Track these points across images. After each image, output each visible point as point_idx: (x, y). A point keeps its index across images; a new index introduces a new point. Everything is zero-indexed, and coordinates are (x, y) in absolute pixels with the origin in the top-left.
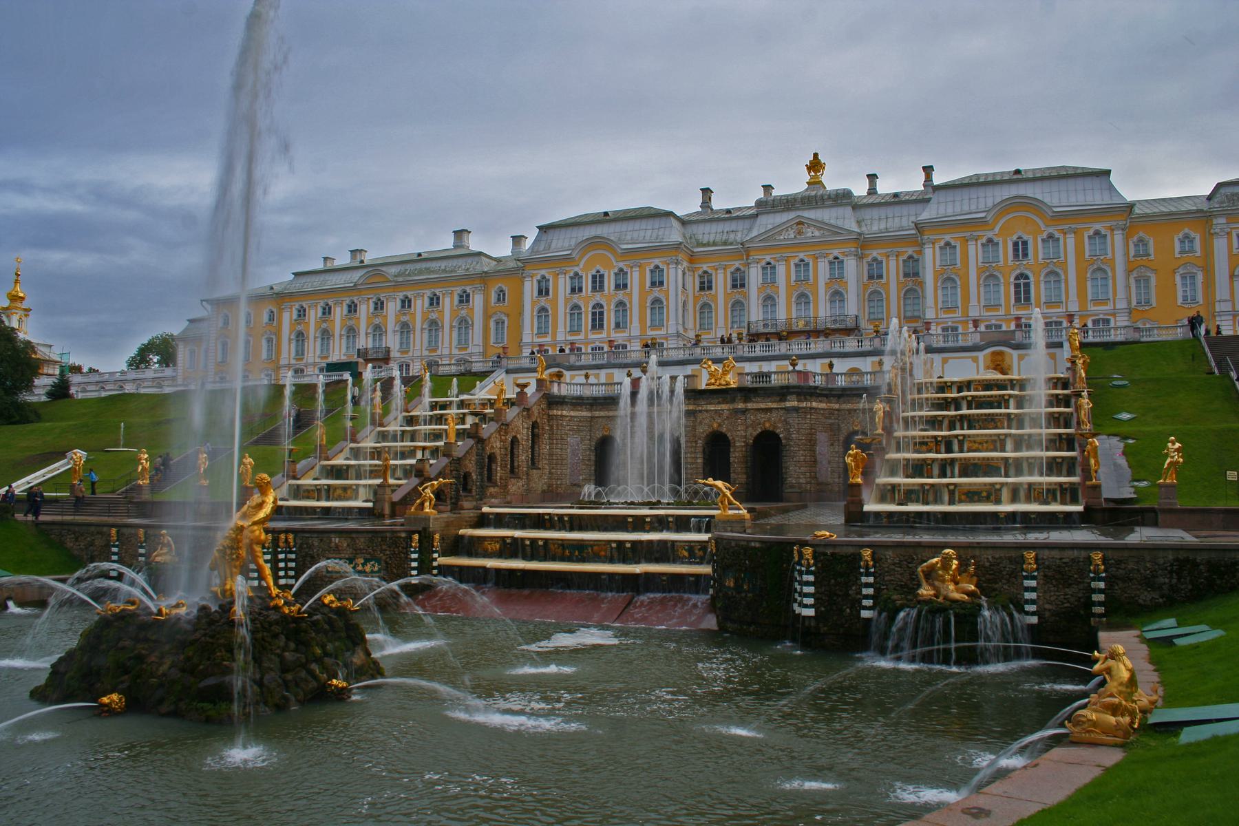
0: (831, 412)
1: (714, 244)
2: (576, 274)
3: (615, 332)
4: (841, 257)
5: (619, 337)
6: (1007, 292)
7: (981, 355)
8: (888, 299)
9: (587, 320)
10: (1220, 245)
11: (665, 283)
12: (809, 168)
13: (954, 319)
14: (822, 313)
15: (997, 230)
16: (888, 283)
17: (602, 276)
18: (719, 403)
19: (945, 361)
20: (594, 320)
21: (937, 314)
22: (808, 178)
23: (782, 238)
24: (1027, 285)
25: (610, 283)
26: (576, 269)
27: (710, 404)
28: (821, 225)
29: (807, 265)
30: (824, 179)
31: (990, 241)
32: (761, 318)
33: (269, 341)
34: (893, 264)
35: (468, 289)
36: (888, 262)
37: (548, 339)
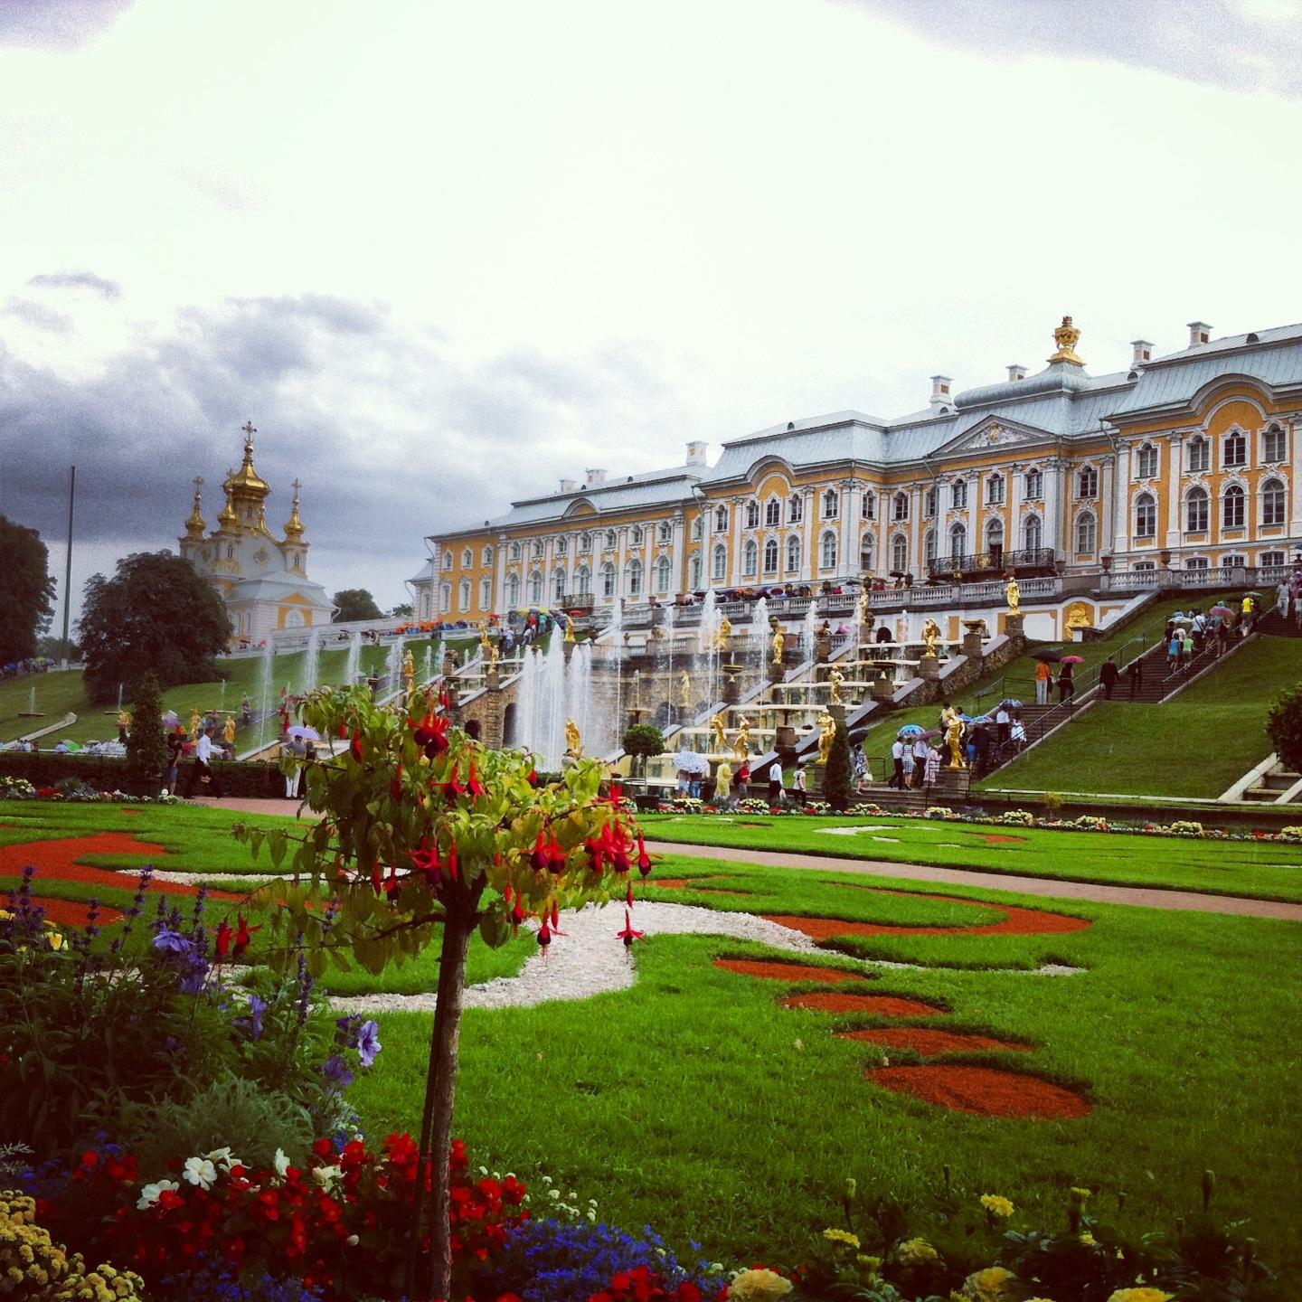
4: (1038, 469)
7: (1059, 608)
13: (1151, 553)
15: (1206, 424)
17: (777, 506)
20: (768, 560)
21: (1129, 548)
23: (974, 446)
24: (1240, 501)
25: (786, 513)
26: (752, 497)
28: (1016, 427)
29: (1003, 480)
30: (1080, 351)
33: (487, 585)
36: (1102, 470)
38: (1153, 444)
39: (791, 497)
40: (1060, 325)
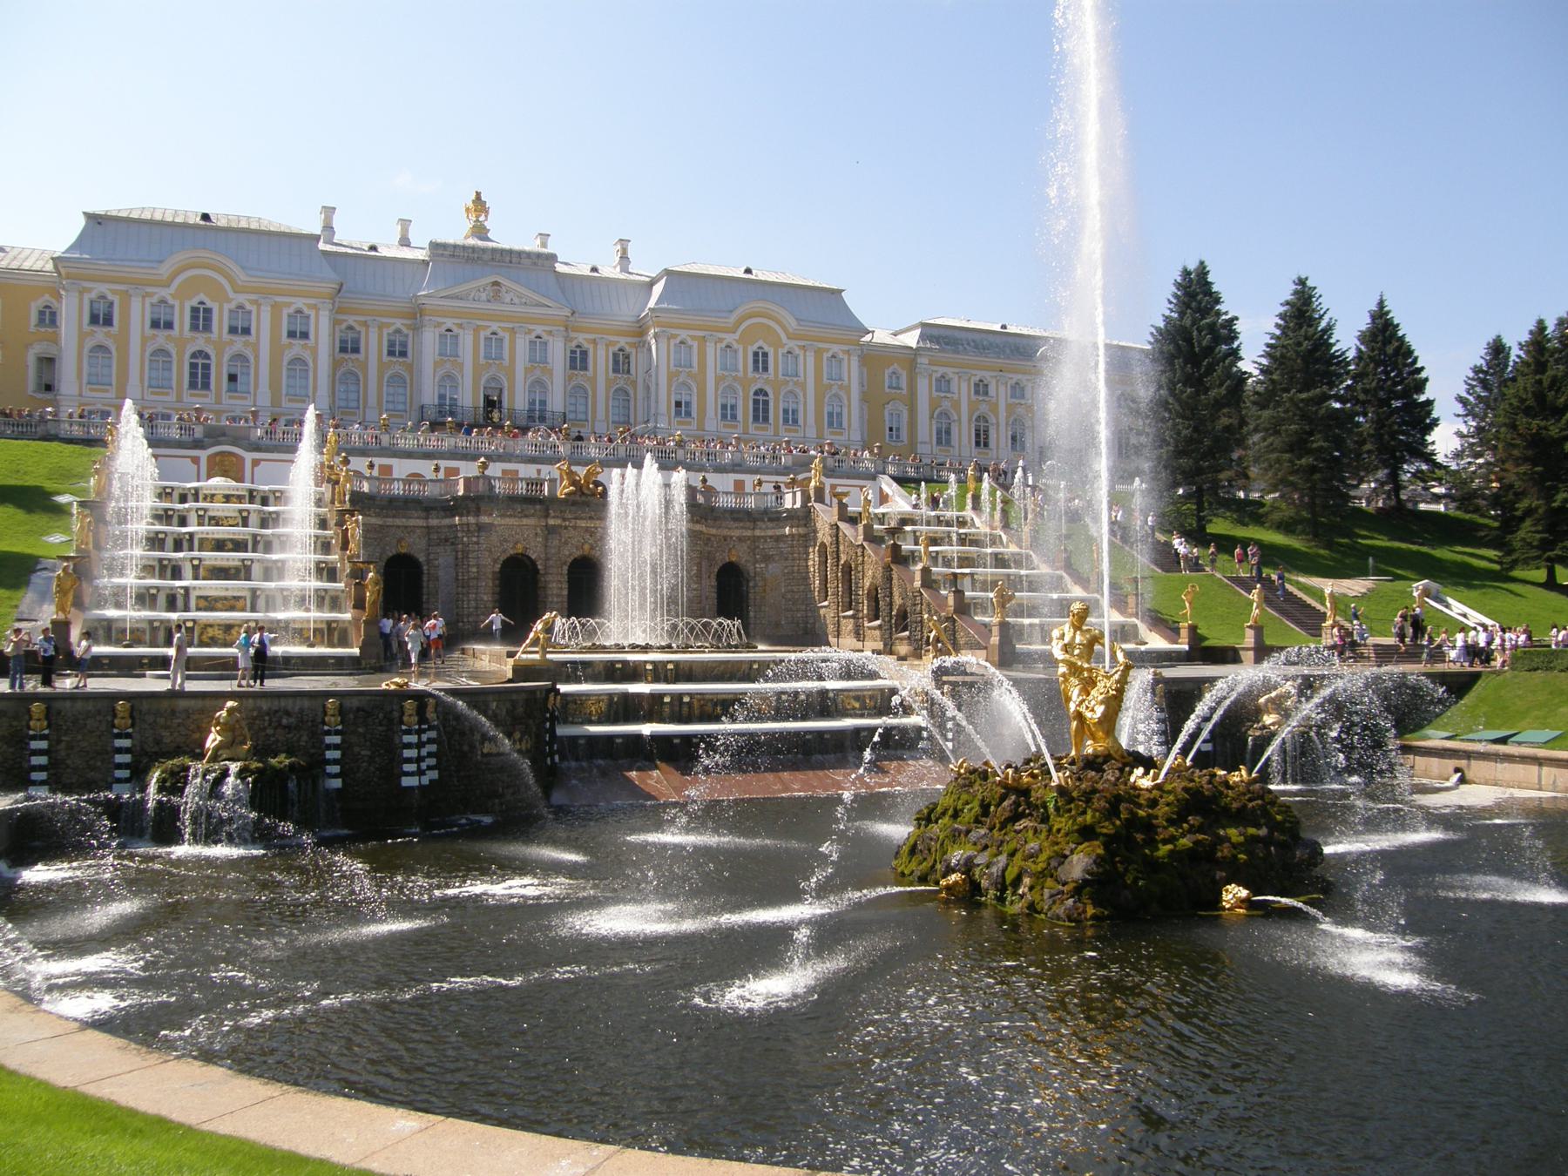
2: (163, 301)
3: (230, 397)
4: (545, 337)
5: (239, 404)
6: (744, 409)
8: (595, 396)
9: (181, 372)
10: (923, 387)
11: (312, 336)
12: (468, 210)
15: (738, 333)
16: (594, 379)
17: (208, 311)
18: (591, 518)
20: (193, 375)
24: (766, 403)
25: (220, 322)
26: (165, 293)
27: (581, 519)
29: (501, 340)
32: (436, 402)
34: (601, 352)
38: (690, 342)
39: (233, 305)
40: (473, 196)
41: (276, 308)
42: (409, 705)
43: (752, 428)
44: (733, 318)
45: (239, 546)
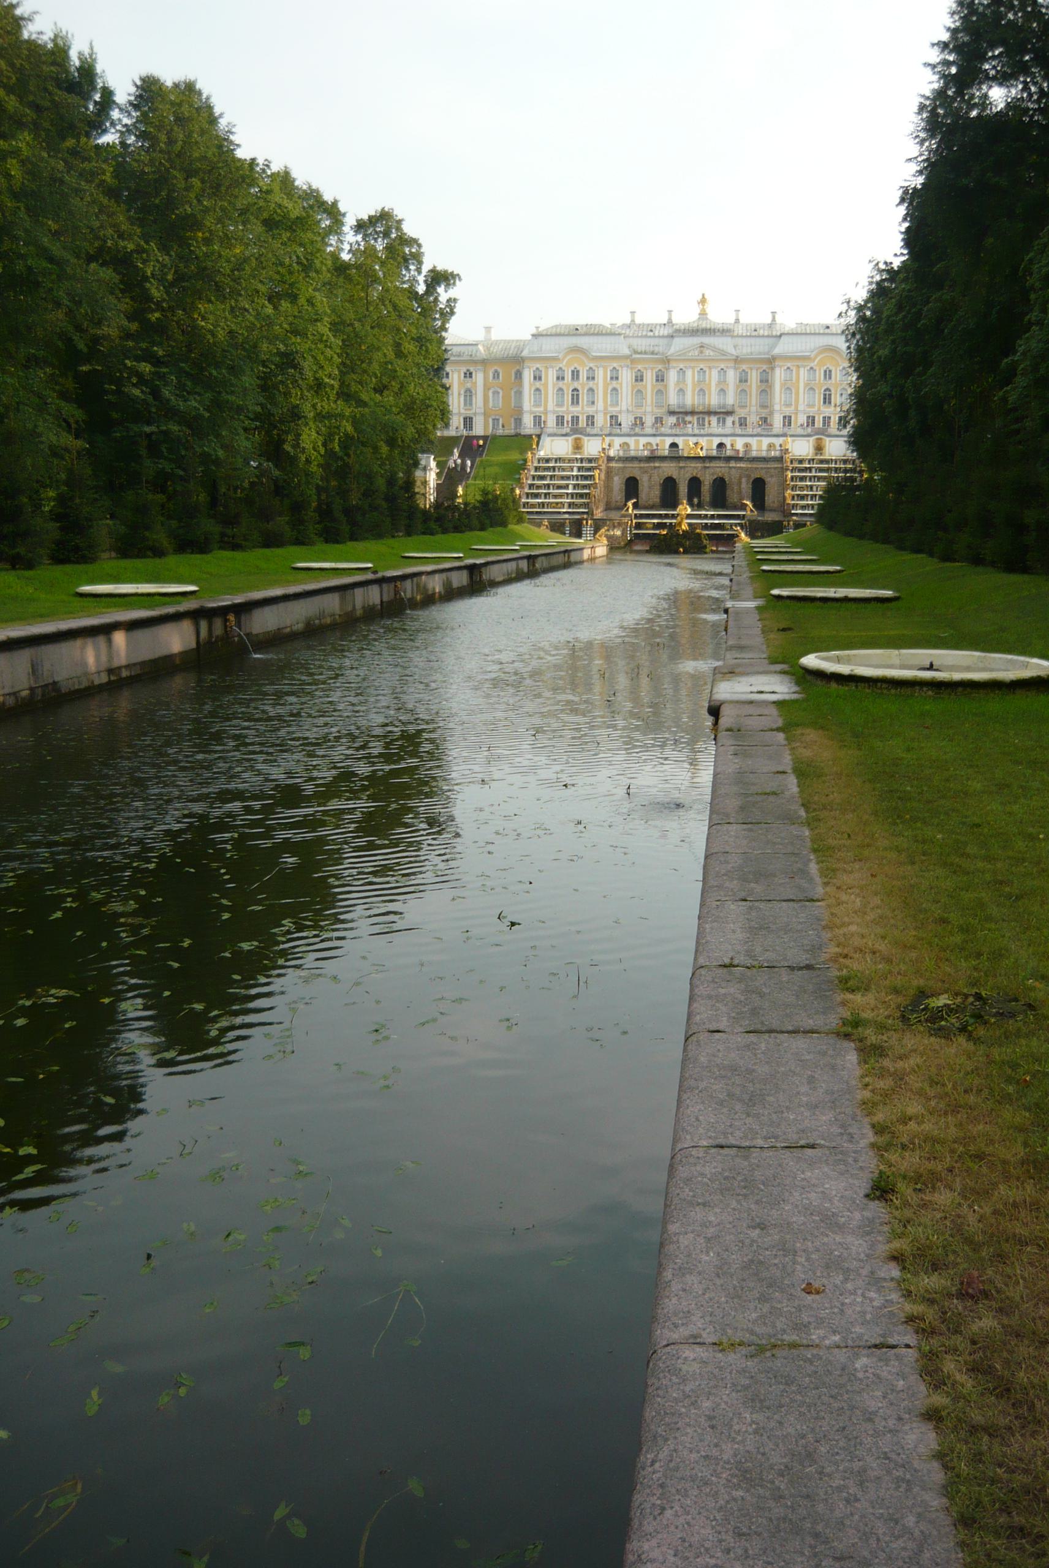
0: (747, 469)
1: (646, 353)
2: (560, 368)
5: (591, 410)
6: (819, 398)
9: (568, 398)
14: (712, 403)
15: (816, 363)
17: (578, 371)
19: (793, 441)
20: (573, 399)
22: (699, 311)
24: (830, 395)
25: (583, 375)
26: (561, 365)
28: (714, 349)
29: (705, 372)
31: (812, 368)
35: (472, 369)
37: (542, 409)
40: (701, 297)
41: (605, 368)
42: (585, 522)
43: (822, 408)
44: (813, 355)
45: (568, 478)
